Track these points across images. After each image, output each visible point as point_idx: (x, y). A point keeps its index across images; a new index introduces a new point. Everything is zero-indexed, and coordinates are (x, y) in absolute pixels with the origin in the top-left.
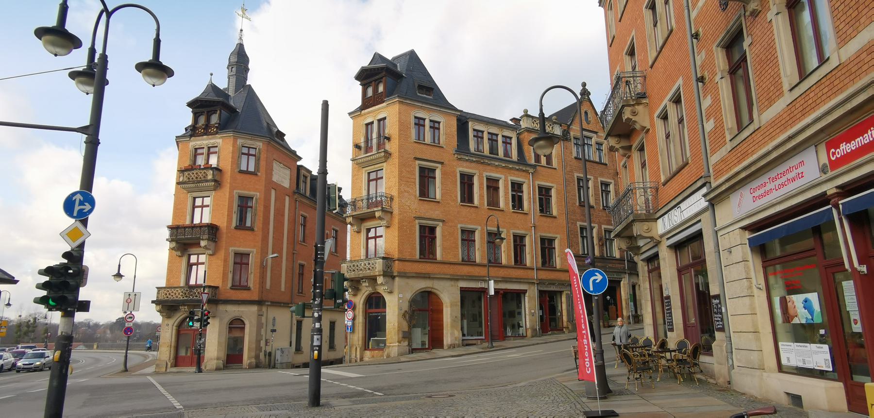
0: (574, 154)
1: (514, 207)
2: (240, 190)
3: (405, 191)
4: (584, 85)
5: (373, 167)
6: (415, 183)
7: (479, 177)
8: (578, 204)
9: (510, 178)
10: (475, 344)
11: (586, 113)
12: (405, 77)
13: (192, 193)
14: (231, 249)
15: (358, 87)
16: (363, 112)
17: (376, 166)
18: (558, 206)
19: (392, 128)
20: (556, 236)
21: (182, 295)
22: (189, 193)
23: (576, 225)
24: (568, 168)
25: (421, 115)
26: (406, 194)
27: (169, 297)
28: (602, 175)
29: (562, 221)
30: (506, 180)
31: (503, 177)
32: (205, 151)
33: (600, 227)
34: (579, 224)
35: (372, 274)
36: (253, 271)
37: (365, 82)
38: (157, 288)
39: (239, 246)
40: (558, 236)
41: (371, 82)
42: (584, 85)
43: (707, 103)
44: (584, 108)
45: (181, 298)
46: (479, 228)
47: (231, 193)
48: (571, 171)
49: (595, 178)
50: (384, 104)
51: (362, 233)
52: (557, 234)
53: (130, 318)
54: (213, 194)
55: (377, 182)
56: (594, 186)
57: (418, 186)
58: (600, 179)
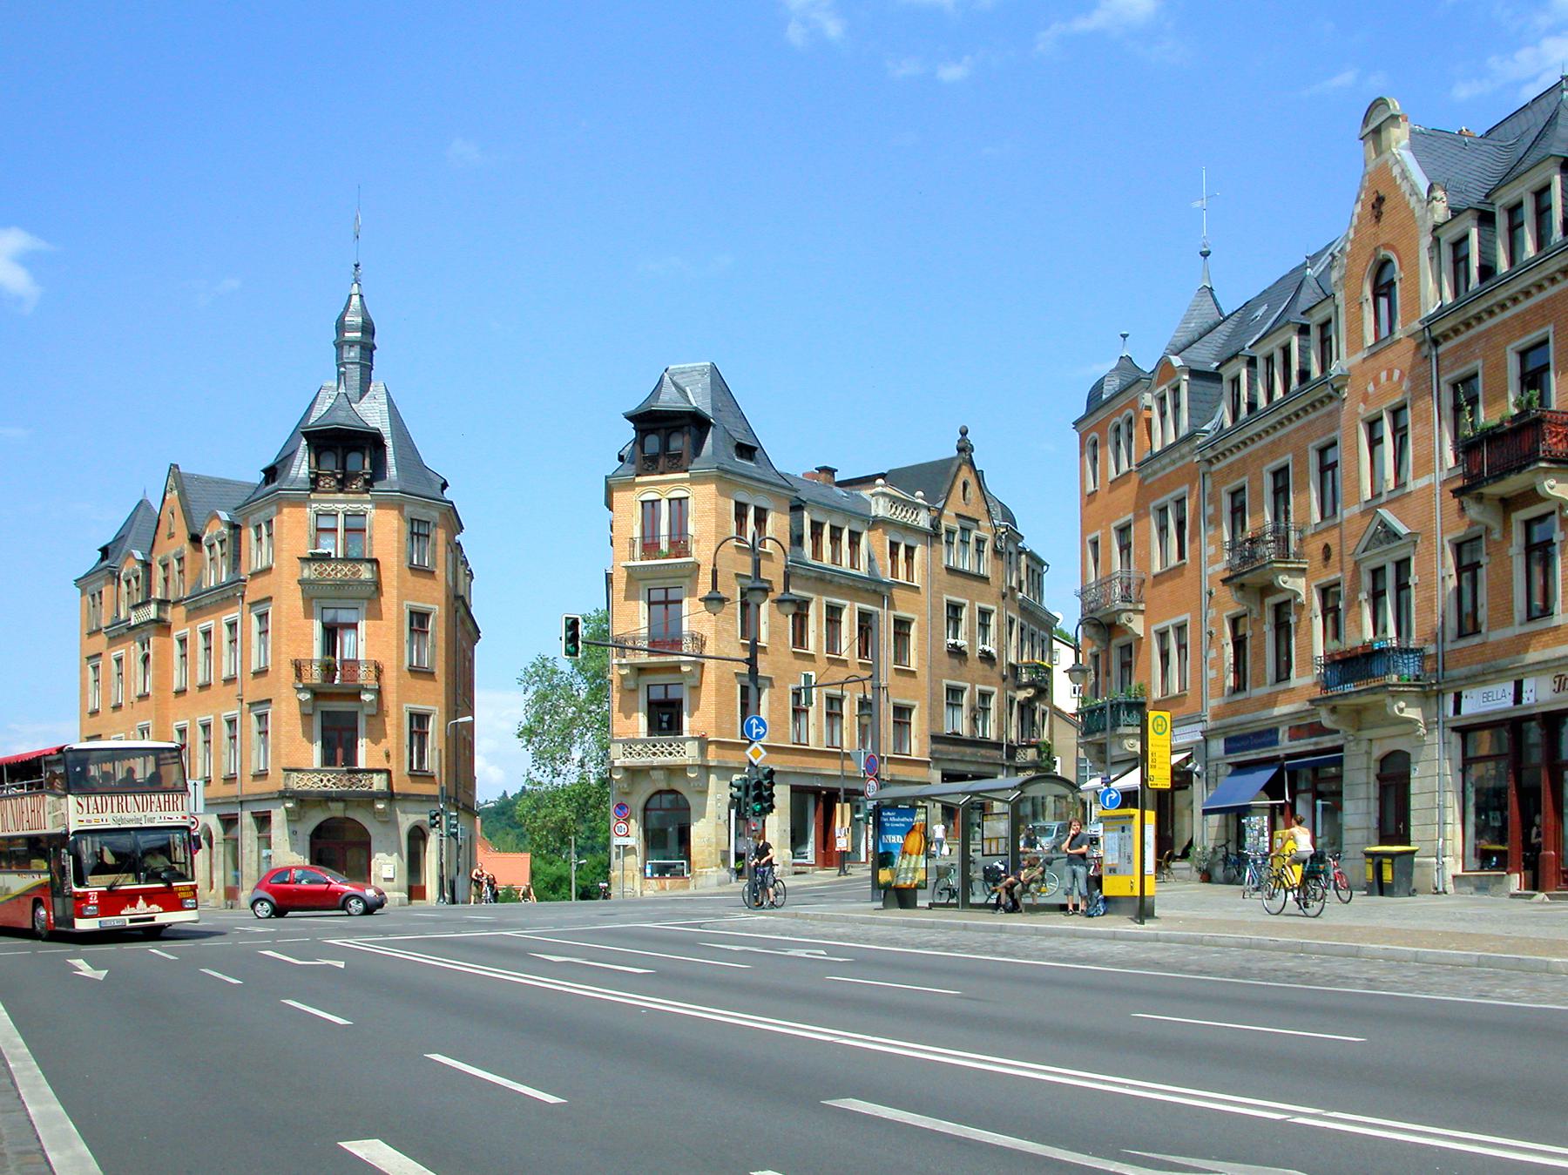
0: (945, 562)
1: (860, 657)
2: (414, 600)
3: (724, 629)
4: (964, 433)
5: (661, 581)
6: (736, 616)
7: (817, 603)
9: (857, 605)
10: (804, 873)
11: (965, 485)
12: (714, 426)
14: (405, 706)
15: (629, 432)
16: (638, 479)
17: (668, 581)
24: (936, 586)
25: (743, 499)
26: (725, 635)
27: (330, 784)
28: (981, 600)
29: (924, 677)
30: (852, 609)
31: (848, 603)
33: (973, 688)
34: (945, 682)
35: (679, 763)
36: (436, 745)
37: (646, 426)
39: (415, 703)
41: (658, 429)
42: (964, 433)
43: (1213, 654)
44: (965, 475)
45: (335, 789)
47: (400, 605)
49: (972, 603)
50: (686, 475)
52: (915, 698)
54: (365, 605)
55: (666, 608)
56: (970, 617)
57: (739, 621)
58: (977, 604)
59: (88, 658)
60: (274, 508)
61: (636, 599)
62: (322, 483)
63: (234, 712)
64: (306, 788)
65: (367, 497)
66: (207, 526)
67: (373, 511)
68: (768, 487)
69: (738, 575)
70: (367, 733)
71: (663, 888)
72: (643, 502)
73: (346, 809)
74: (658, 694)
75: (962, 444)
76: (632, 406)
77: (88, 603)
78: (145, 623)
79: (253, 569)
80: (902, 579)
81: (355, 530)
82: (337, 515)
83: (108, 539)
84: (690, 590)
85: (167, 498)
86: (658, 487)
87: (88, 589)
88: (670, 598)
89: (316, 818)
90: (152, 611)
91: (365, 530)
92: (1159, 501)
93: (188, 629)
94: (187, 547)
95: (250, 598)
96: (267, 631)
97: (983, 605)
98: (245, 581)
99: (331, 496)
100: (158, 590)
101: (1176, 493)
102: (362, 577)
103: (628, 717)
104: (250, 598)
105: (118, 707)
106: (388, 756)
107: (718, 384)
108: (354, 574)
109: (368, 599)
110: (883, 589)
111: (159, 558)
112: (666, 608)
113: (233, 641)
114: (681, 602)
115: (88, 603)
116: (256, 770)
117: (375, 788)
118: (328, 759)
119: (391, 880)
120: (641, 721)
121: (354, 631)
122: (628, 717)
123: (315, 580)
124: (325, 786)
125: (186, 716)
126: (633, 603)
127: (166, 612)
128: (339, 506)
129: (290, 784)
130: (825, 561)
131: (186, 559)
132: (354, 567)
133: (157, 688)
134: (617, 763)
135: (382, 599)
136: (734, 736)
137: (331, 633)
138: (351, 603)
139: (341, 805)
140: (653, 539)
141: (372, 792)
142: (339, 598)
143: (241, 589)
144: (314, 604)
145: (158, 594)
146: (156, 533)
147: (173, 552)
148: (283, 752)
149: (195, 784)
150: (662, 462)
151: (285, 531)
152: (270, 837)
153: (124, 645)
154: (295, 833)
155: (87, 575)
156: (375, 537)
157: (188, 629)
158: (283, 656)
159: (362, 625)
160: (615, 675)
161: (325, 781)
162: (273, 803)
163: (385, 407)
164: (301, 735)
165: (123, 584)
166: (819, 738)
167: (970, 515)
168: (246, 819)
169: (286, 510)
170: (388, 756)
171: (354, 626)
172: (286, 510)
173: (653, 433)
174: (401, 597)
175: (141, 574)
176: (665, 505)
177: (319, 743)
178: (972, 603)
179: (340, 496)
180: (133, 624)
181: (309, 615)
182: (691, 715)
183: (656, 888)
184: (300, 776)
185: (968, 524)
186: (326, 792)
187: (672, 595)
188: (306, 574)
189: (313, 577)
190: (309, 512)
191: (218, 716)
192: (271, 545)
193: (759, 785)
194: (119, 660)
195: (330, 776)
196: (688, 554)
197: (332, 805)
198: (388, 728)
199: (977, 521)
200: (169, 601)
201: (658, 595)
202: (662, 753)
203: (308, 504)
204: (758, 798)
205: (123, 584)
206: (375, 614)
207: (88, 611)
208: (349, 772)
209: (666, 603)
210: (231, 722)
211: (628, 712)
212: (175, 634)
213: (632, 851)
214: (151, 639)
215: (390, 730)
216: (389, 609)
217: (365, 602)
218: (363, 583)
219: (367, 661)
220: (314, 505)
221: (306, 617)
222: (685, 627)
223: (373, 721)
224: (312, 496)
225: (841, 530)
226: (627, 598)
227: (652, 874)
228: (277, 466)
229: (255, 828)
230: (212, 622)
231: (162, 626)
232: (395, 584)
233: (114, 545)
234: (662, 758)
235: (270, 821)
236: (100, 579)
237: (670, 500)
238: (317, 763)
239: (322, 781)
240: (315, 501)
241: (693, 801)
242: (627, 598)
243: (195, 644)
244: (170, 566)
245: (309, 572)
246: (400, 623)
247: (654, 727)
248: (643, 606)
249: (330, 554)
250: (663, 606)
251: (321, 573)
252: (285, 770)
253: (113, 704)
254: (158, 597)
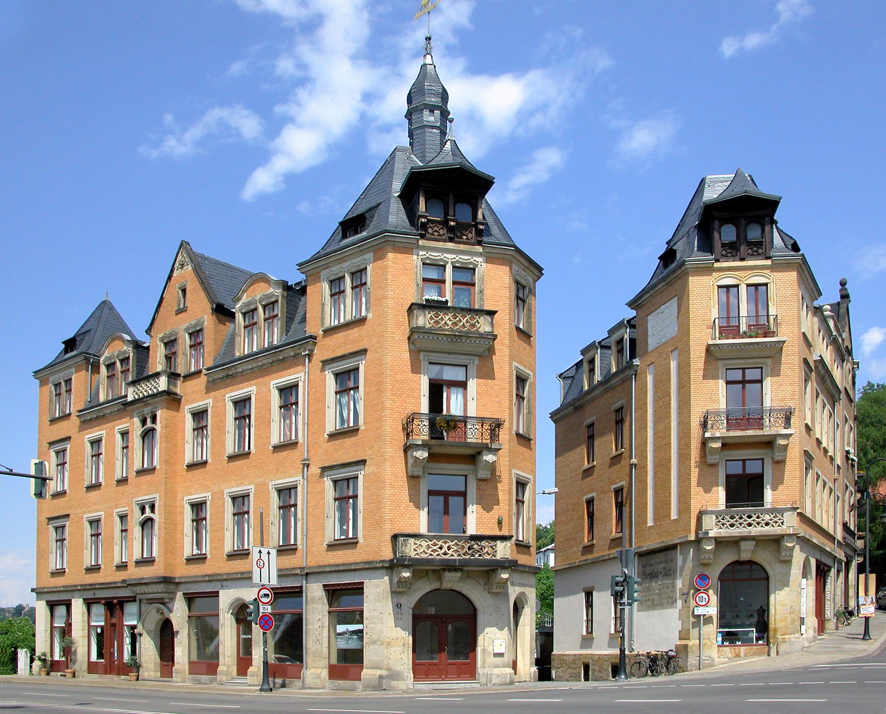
13: (428, 354)
21: (456, 551)
22: (422, 354)
51: (720, 467)
54: (476, 362)
55: (744, 387)
59: (51, 444)
60: (370, 256)
61: (715, 377)
62: (430, 231)
64: (424, 556)
66: (244, 291)
67: (484, 265)
68: (812, 285)
70: (477, 499)
71: (738, 656)
74: (737, 469)
75: (844, 293)
77: (51, 392)
78: (154, 396)
79: (327, 325)
82: (445, 266)
83: (71, 335)
84: (772, 370)
85: (175, 275)
86: (737, 273)
87: (51, 379)
88: (747, 378)
91: (473, 285)
93: (210, 401)
94: (208, 320)
96: (358, 388)
98: (315, 338)
99: (440, 245)
102: (481, 330)
103: (707, 491)
105: (94, 487)
106: (500, 523)
109: (479, 356)
111: (161, 335)
112: (744, 387)
114: (760, 381)
115: (51, 392)
116: (332, 540)
117: (498, 557)
119: (501, 655)
120: (721, 493)
121: (460, 390)
122: (707, 491)
123: (430, 329)
124: (445, 554)
125: (205, 488)
126: (712, 382)
127: (175, 386)
128: (447, 255)
129: (407, 551)
131: (206, 331)
133: (166, 462)
135: (494, 357)
137: (436, 390)
138: (462, 360)
140: (728, 322)
141: (497, 561)
142: (449, 353)
143: (310, 347)
144: (421, 358)
146: (157, 311)
147: (185, 326)
148: (387, 517)
149: (269, 553)
150: (743, 248)
151: (389, 277)
152: (363, 611)
153: (105, 426)
154: (398, 606)
155: (50, 366)
157: (210, 401)
158: (387, 412)
159: (472, 384)
161: (445, 549)
162: (365, 573)
164: (407, 498)
165: (103, 369)
168: (315, 591)
169: (390, 256)
170: (500, 523)
171: (463, 385)
172: (390, 256)
173: (728, 223)
174: (512, 357)
175: (131, 355)
176: (743, 289)
177: (426, 509)
179: (450, 245)
181: (416, 368)
182: (774, 489)
183: (730, 656)
184: (418, 542)
187: (751, 374)
189: (428, 326)
190: (415, 260)
192: (357, 298)
194: (96, 442)
196: (773, 334)
198: (500, 494)
200: (179, 375)
201: (737, 375)
202: (776, 522)
203: (415, 251)
205: (103, 369)
206: (487, 373)
207: (51, 400)
209: (744, 382)
210: (286, 492)
211: (707, 486)
212: (186, 407)
213: (708, 620)
214: (159, 413)
215: (502, 496)
216: (501, 368)
217: (477, 360)
219: (482, 420)
220: (421, 253)
221: (413, 372)
222: (767, 403)
223: (484, 486)
224: (421, 242)
226: (705, 377)
227: (723, 643)
228: (367, 215)
229: (326, 601)
230: (254, 388)
231: (172, 399)
232: (507, 342)
233: (81, 337)
234: (759, 528)
235: (363, 594)
236: (69, 367)
240: (424, 248)
241: (774, 569)
242: (705, 377)
244: (180, 341)
245: (423, 320)
246: (511, 382)
247: (733, 498)
248: (722, 383)
249: (447, 302)
250: (741, 385)
251: (437, 322)
253: (86, 484)
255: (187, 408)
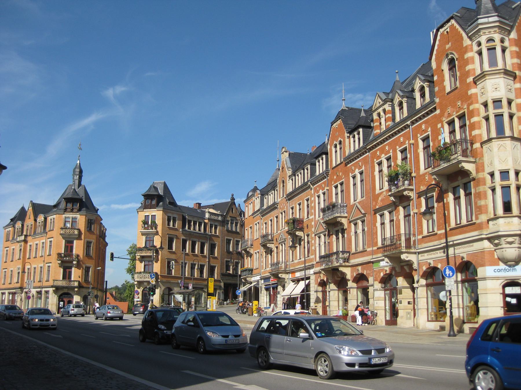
4: (233, 195)
6: (166, 244)
8: (225, 251)
15: (142, 198)
16: (144, 210)
18: (218, 254)
19: (159, 221)
20: (216, 265)
23: (224, 260)
25: (170, 215)
28: (236, 238)
32: (71, 220)
34: (225, 259)
38: (53, 280)
40: (217, 265)
42: (233, 195)
45: (65, 285)
46: (188, 262)
48: (224, 236)
49: (234, 239)
50: (156, 210)
52: (216, 264)
53: (30, 292)
63: (42, 265)
65: (78, 213)
69: (168, 234)
72: (145, 216)
73: (68, 290)
76: (143, 193)
80: (213, 233)
81: (74, 221)
89: (61, 292)
90: (23, 238)
92: (256, 223)
95: (48, 236)
97: (237, 239)
100: (25, 232)
101: (258, 222)
104: (48, 236)
107: (166, 187)
108: (73, 233)
110: (208, 236)
113: (43, 247)
118: (64, 278)
127: (27, 238)
130: (192, 230)
132: (73, 231)
134: (136, 280)
136: (165, 274)
139: (67, 289)
145: (25, 233)
156: (79, 224)
160: (138, 257)
163: (84, 191)
166: (188, 274)
167: (234, 216)
178: (234, 239)
179: (71, 213)
180: (18, 240)
185: (233, 219)
186: (63, 286)
188: (62, 232)
191: (38, 266)
193: (152, 288)
195: (64, 282)
197: (64, 289)
199: (236, 218)
204: (152, 292)
208: (69, 281)
218: (75, 235)
225: (196, 222)
237: (152, 215)
238: (61, 279)
239: (62, 283)
243: (33, 247)
252: (53, 280)
254: (25, 234)
255: (29, 244)
